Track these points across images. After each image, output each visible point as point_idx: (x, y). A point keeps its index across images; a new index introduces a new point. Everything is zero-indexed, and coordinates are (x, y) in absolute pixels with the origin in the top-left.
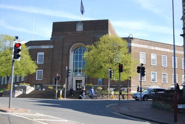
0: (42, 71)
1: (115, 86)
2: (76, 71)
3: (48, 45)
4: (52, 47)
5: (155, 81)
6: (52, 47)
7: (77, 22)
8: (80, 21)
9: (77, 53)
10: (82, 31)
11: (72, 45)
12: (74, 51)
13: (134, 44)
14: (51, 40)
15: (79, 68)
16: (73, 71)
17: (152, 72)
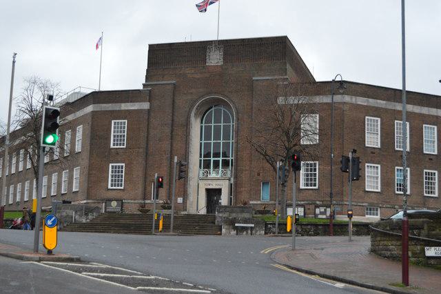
0: (122, 167)
1: (302, 203)
2: (207, 165)
3: (137, 102)
4: (145, 106)
5: (434, 194)
6: (145, 106)
7: (210, 43)
8: (215, 41)
9: (209, 121)
10: (221, 66)
11: (197, 100)
12: (203, 114)
13: (351, 98)
14: (146, 89)
15: (216, 159)
16: (200, 167)
17: (396, 168)
